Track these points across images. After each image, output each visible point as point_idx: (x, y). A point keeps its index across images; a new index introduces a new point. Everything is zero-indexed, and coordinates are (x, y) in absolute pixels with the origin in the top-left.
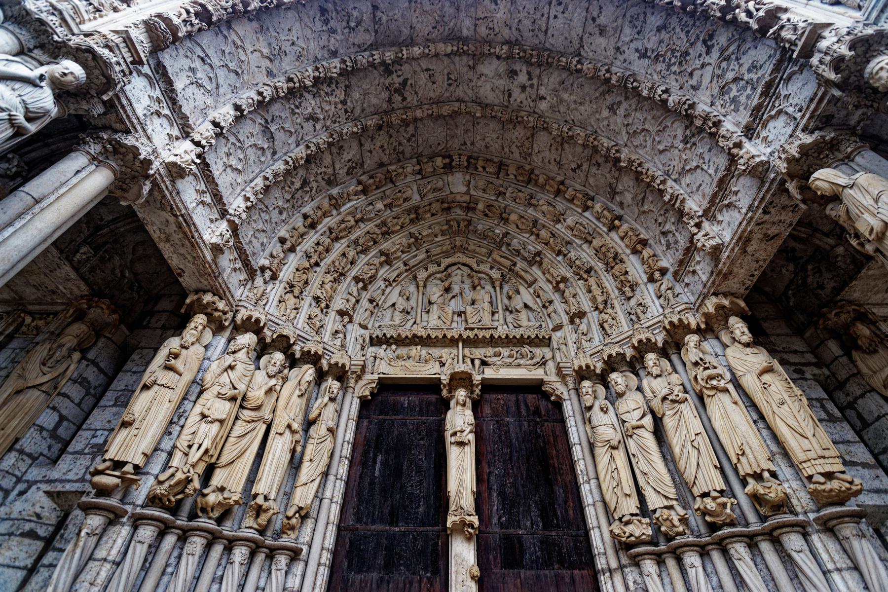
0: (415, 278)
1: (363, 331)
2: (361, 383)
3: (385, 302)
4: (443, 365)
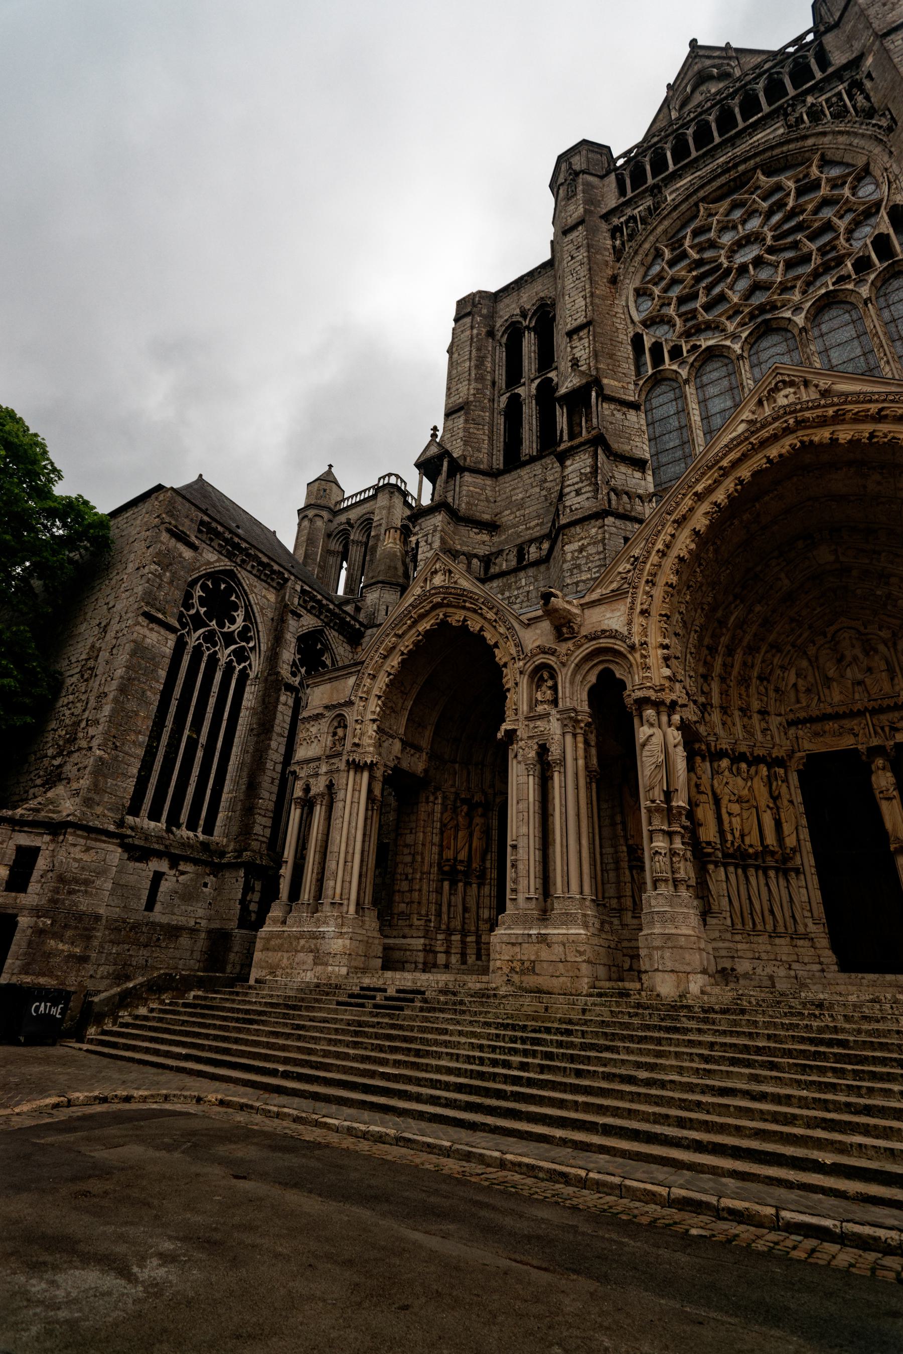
0: (805, 653)
1: (779, 718)
2: (793, 761)
3: (786, 685)
4: (856, 735)
